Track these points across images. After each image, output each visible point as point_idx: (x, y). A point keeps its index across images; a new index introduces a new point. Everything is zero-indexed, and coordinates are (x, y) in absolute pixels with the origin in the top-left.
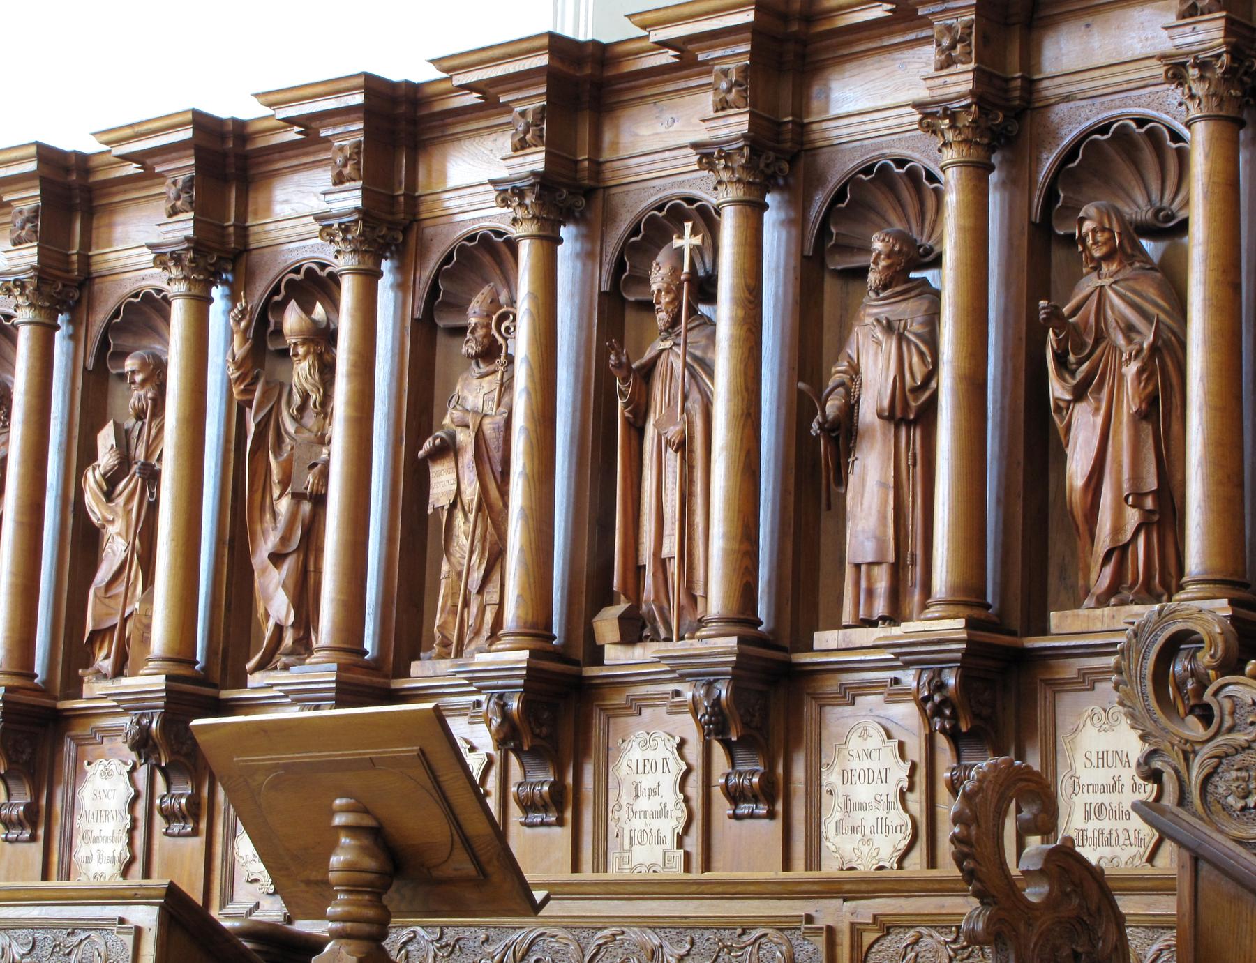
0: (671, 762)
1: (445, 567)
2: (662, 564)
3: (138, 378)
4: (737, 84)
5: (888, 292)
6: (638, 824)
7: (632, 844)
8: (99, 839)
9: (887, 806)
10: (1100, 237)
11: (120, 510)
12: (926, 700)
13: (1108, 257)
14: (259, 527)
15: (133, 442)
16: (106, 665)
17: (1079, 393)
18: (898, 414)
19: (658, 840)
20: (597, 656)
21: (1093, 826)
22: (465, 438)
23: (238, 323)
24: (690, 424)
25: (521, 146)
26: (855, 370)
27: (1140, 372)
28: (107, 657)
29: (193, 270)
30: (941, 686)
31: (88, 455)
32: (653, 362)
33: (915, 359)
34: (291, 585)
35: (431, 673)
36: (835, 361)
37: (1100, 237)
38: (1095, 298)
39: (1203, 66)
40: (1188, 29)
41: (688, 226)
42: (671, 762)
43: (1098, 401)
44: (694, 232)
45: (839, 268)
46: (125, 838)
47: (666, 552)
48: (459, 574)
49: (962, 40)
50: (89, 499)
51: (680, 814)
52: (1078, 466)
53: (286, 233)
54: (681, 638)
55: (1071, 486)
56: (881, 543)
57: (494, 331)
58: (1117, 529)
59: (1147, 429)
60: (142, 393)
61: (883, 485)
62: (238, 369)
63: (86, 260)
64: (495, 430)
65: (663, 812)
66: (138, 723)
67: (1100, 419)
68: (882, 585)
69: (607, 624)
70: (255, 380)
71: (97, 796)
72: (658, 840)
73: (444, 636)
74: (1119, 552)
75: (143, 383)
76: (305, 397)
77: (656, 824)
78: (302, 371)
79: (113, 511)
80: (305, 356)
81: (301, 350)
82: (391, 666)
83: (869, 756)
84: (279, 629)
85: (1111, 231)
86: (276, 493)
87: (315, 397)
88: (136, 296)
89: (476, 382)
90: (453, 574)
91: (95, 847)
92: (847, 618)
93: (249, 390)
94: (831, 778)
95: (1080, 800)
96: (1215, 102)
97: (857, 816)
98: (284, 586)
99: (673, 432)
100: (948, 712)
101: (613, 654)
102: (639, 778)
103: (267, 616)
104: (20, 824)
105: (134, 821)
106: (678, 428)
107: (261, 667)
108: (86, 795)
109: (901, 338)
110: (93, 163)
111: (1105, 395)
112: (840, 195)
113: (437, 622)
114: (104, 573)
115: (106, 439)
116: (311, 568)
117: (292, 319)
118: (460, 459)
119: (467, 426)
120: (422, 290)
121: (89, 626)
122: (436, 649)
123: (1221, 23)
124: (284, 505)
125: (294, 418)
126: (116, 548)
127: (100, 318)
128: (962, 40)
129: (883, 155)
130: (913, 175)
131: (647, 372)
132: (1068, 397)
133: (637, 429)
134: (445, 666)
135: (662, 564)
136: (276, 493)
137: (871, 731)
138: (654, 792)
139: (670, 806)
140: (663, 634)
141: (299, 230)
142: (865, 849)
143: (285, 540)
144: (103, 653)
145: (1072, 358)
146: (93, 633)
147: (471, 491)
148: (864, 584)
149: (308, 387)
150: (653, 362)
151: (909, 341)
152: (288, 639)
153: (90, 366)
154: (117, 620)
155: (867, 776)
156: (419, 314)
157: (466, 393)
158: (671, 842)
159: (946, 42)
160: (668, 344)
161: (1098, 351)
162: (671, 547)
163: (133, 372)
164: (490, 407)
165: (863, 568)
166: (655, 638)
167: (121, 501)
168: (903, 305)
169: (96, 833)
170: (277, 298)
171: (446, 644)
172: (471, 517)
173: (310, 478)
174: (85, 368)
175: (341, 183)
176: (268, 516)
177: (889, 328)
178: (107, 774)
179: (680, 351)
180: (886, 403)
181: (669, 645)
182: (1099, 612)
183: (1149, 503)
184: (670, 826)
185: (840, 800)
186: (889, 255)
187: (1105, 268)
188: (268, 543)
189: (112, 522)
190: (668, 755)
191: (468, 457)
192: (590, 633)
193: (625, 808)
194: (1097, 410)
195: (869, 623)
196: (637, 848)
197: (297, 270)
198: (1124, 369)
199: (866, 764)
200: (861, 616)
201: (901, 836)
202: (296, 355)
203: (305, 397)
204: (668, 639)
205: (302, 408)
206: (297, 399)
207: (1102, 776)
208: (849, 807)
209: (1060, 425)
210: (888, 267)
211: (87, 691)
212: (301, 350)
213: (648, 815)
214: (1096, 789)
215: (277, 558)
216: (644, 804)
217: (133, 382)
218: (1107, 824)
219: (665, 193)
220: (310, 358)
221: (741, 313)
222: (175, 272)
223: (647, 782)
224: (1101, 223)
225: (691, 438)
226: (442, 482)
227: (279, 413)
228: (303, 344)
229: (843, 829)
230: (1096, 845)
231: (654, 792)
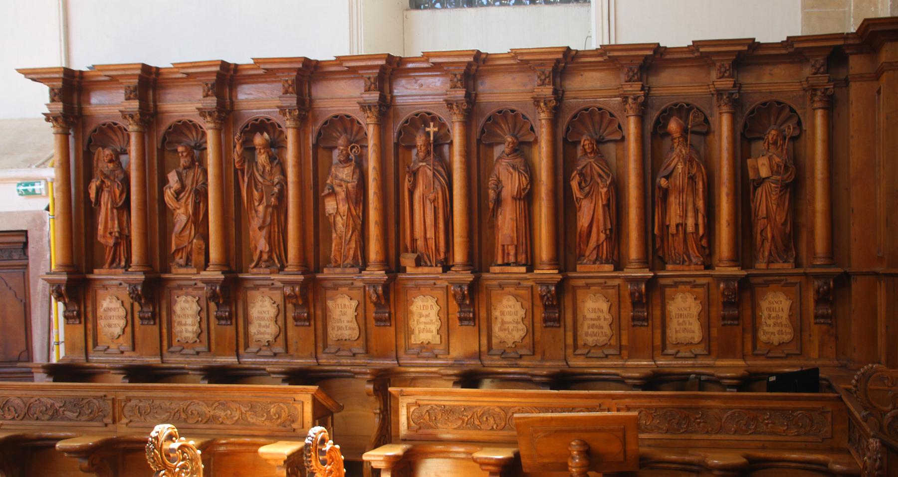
0: (434, 307)
1: (334, 235)
2: (426, 239)
3: (185, 154)
4: (460, 80)
5: (512, 155)
6: (422, 326)
7: (419, 332)
8: (185, 325)
9: (517, 323)
10: (590, 146)
11: (183, 205)
12: (544, 296)
13: (591, 153)
14: (250, 216)
15: (184, 178)
16: (182, 262)
17: (586, 196)
18: (518, 197)
19: (430, 331)
20: (404, 270)
21: (590, 331)
22: (338, 189)
23: (238, 140)
24: (438, 194)
25: (368, 90)
26: (499, 181)
27: (607, 191)
28: (181, 258)
29: (216, 119)
30: (549, 292)
31: (164, 181)
32: (418, 169)
33: (524, 179)
34: (267, 237)
35: (333, 272)
36: (489, 176)
37: (590, 146)
38: (589, 166)
39: (635, 99)
40: (629, 86)
41: (432, 124)
42: (434, 307)
43: (592, 199)
44: (434, 126)
45: (487, 143)
46: (197, 325)
47: (428, 236)
48: (340, 238)
49: (548, 77)
50: (167, 199)
51: (439, 323)
52: (583, 221)
53: (252, 106)
54: (436, 266)
55: (582, 226)
56: (512, 238)
57: (350, 152)
58: (598, 240)
59: (607, 209)
60: (186, 159)
61: (512, 219)
62: (239, 157)
63: (156, 106)
64: (353, 188)
65: (431, 322)
66: (211, 289)
67: (592, 206)
68: (512, 252)
69: (408, 260)
70: (244, 162)
71: (183, 309)
72: (430, 331)
73: (336, 260)
74: (598, 247)
75: (186, 156)
76: (264, 167)
77: (428, 326)
78: (262, 158)
79: (180, 205)
80: (264, 153)
81: (262, 151)
82: (313, 268)
83: (510, 307)
84: (261, 252)
85: (593, 144)
86: (256, 204)
87: (268, 168)
88: (180, 122)
89: (341, 169)
90: (338, 238)
91: (184, 328)
92: (500, 262)
93: (243, 165)
94: (496, 313)
95: (586, 323)
96: (638, 111)
97: (506, 326)
98: (265, 238)
99: (432, 196)
100: (551, 299)
101: (409, 270)
102: (421, 311)
103: (256, 248)
104: (149, 319)
105: (201, 318)
106: (433, 195)
107: (255, 266)
108: (178, 308)
109: (519, 172)
110: (161, 71)
111: (594, 197)
112: (489, 119)
113: (333, 254)
114: (178, 228)
115: (173, 177)
116: (272, 230)
117: (259, 140)
118: (338, 197)
119: (341, 186)
120: (315, 134)
121: (174, 248)
122: (333, 264)
123: (641, 86)
124: (261, 208)
125: (261, 176)
126: (181, 216)
127: (163, 129)
128: (548, 77)
129: (507, 108)
130: (516, 116)
131: (414, 174)
132: (582, 197)
133: (411, 193)
134: (338, 270)
135: (426, 239)
136: (256, 204)
137: (511, 299)
138: (427, 316)
139: (434, 321)
140: (429, 264)
141: (258, 106)
142: (510, 336)
143: (264, 222)
144: (180, 256)
145: (583, 184)
146: (176, 251)
147: (343, 208)
148: (506, 251)
149: (265, 164)
150: (418, 169)
151: (521, 172)
152: (265, 257)
153: (160, 147)
154: (186, 244)
155: (510, 313)
156: (314, 142)
157: (337, 173)
158: (435, 332)
159: (543, 77)
160: (424, 164)
161: (591, 184)
162: (430, 234)
163: (182, 152)
164: (349, 179)
165: (506, 246)
166: (426, 265)
167: (183, 200)
168: (516, 160)
169: (184, 322)
170: (246, 129)
171: (336, 261)
172: (345, 218)
173: (273, 200)
174: (158, 149)
175: (286, 93)
176: (254, 212)
177: (514, 167)
178: (187, 301)
179: (432, 169)
180: (515, 193)
181: (432, 268)
182: (593, 266)
183: (608, 232)
184: (434, 327)
185: (499, 320)
186: (513, 143)
187: (589, 155)
188: (256, 223)
189: (179, 209)
190: (433, 304)
191: (342, 195)
192: (398, 261)
193: (416, 321)
194: (592, 202)
195: (508, 264)
196: (421, 334)
197: (257, 120)
198: (601, 190)
199: (509, 309)
200: (506, 261)
201: (522, 332)
202: (260, 152)
203: (264, 167)
204: (431, 266)
205: (263, 172)
206: (261, 168)
207: (593, 315)
208: (503, 323)
209: (578, 206)
210: (512, 147)
211: (173, 270)
212: (262, 151)
213: (425, 323)
214: (592, 319)
215: (261, 228)
216: (423, 320)
217: (182, 155)
218: (595, 330)
219: (420, 110)
220: (266, 153)
221: (464, 160)
222: (209, 119)
223: (424, 312)
224: (591, 142)
225: (438, 198)
226: (330, 206)
227: (254, 173)
228: (264, 148)
229: (501, 329)
230: (592, 336)
231: (427, 316)
